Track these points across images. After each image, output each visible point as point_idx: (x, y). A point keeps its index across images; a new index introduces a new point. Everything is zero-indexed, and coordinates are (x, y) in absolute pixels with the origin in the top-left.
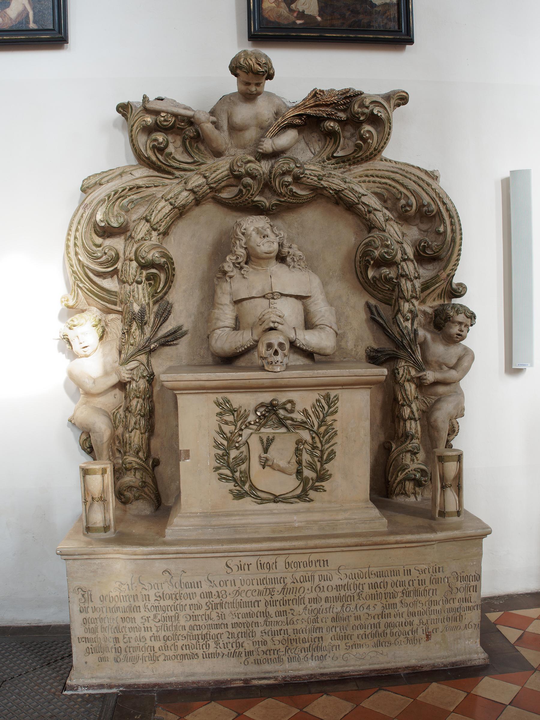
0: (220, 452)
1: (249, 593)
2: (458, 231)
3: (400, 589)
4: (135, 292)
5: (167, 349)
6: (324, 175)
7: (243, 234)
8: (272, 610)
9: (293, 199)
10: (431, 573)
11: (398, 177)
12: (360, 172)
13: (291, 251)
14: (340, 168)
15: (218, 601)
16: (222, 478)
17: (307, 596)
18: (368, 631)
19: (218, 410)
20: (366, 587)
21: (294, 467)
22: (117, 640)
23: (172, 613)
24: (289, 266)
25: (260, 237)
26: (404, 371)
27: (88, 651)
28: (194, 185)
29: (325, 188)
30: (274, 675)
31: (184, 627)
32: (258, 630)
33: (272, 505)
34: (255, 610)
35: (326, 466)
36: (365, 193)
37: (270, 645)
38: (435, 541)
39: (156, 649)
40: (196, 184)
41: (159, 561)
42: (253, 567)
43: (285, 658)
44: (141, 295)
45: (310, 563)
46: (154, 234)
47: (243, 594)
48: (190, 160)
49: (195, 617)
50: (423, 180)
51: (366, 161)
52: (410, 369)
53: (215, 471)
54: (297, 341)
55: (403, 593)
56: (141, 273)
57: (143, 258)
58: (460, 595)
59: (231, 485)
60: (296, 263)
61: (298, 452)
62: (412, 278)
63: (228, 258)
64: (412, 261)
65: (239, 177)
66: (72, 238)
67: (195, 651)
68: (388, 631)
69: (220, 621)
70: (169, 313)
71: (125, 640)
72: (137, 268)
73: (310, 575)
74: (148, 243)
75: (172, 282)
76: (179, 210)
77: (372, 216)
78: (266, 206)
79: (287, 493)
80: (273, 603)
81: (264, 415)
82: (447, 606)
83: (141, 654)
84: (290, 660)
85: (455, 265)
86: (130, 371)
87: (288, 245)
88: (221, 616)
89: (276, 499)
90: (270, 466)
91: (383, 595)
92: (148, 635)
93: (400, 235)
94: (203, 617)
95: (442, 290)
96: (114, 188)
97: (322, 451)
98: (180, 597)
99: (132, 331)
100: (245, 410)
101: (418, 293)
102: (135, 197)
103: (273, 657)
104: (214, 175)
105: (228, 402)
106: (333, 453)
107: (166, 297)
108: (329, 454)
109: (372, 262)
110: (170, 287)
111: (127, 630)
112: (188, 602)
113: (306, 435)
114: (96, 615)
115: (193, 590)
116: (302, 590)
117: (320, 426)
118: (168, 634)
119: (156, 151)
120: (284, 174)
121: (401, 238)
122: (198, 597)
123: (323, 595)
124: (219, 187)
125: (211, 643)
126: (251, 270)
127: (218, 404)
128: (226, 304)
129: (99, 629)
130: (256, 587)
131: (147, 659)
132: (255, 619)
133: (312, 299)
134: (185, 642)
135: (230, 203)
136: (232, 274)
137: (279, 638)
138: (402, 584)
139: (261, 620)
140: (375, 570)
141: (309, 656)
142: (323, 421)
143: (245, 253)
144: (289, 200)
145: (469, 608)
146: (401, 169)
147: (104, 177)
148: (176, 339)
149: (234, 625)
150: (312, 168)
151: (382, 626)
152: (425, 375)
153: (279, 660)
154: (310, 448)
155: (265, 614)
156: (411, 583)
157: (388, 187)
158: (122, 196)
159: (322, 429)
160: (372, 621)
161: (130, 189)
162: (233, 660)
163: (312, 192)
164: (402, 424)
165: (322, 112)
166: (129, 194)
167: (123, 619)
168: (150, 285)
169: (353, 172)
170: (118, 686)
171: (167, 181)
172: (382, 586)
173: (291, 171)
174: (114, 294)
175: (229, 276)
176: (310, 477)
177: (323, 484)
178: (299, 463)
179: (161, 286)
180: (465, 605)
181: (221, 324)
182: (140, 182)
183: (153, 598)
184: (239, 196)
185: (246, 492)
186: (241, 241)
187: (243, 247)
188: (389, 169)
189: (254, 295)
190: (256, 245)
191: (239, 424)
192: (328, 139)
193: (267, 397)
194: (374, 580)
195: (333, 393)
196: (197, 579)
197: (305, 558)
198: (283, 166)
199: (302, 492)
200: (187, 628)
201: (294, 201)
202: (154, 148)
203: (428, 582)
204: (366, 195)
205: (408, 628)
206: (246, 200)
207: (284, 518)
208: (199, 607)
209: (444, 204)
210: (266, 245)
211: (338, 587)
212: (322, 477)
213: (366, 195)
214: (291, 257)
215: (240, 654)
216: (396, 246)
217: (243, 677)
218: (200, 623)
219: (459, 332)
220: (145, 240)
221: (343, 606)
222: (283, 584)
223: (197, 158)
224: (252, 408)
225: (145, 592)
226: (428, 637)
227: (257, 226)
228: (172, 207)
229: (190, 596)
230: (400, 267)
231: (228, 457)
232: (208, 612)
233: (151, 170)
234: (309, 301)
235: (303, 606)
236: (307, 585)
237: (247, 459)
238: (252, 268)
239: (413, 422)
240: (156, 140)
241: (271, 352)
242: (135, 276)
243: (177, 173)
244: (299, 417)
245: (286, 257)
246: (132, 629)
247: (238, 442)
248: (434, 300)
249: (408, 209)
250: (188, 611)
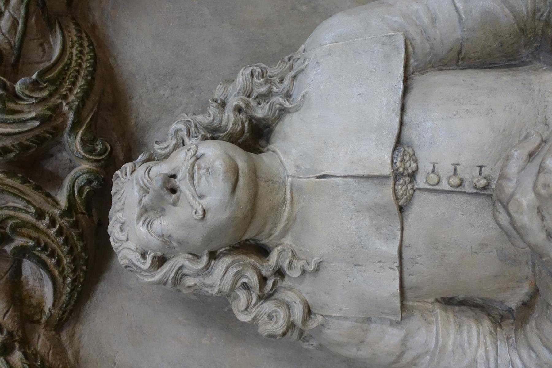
7: (160, 261)
9: (74, 84)
13: (233, 102)
24: (283, 111)
25: (175, 204)
60: (275, 89)
63: (244, 318)
78: (89, 172)
87: (213, 110)
126: (288, 241)
128: (404, 342)
133: (413, 32)
135: (74, 281)
143: (227, 260)
144: (71, 98)
163: (57, 28)
175: (305, 321)
184: (44, 256)
186: (185, 271)
187: (207, 267)
190: (200, 224)
201: (81, 82)
206: (60, 232)
214: (253, 103)
227: (137, 210)
238: (284, 233)
245: (251, 119)
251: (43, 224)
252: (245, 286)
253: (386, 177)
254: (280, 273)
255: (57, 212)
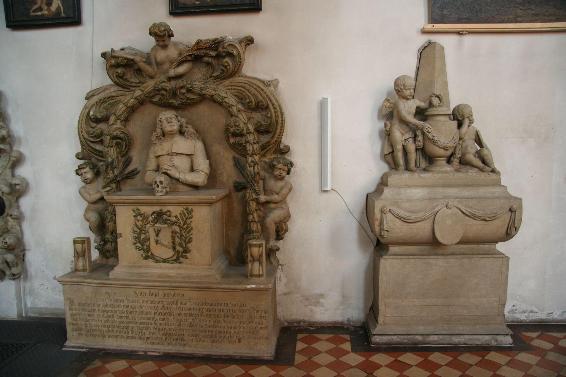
0: (136, 235)
1: (146, 308)
2: (280, 116)
3: (223, 313)
4: (109, 152)
5: (130, 180)
6: (204, 88)
7: (160, 121)
8: (158, 317)
10: (239, 306)
11: (246, 86)
12: (227, 83)
14: (216, 82)
15: (132, 310)
16: (138, 248)
17: (175, 312)
18: (207, 334)
19: (134, 214)
20: (204, 310)
21: (171, 245)
22: (86, 325)
23: (111, 314)
24: (185, 137)
26: (249, 195)
27: (74, 330)
28: (136, 95)
29: (204, 94)
30: (159, 351)
31: (117, 322)
32: (152, 327)
33: (162, 264)
34: (150, 316)
35: (188, 245)
36: (227, 96)
37: (158, 336)
38: (240, 289)
39: (104, 332)
40: (138, 95)
41: (104, 288)
42: (147, 294)
43: (165, 343)
44: (112, 153)
45: (175, 295)
46: (119, 121)
47: (144, 308)
48: (138, 81)
49: (121, 317)
50: (260, 88)
51: (230, 77)
52: (253, 194)
53: (134, 245)
54: (180, 179)
55: (224, 316)
56: (112, 142)
57: (112, 134)
58: (256, 320)
59: (142, 252)
61: (173, 238)
62: (252, 143)
63: (153, 134)
64: (253, 134)
65: (159, 90)
66: (80, 124)
67: (122, 334)
68: (218, 335)
69: (133, 321)
70: (130, 162)
71: (90, 326)
72: (110, 139)
73: (175, 300)
74: (114, 127)
75: (130, 146)
76: (131, 108)
77: (230, 109)
79: (169, 258)
80: (158, 314)
81: (155, 217)
82: (250, 325)
83: (98, 333)
84: (168, 344)
85: (279, 135)
86: (106, 192)
88: (134, 318)
89: (165, 261)
90: (159, 243)
91: (214, 316)
92: (100, 324)
93: (246, 119)
94: (125, 317)
95: (275, 149)
96: (100, 98)
97: (185, 237)
98: (114, 306)
99: (108, 171)
100: (147, 215)
101: (256, 152)
102: (111, 102)
103: (159, 341)
104: (146, 90)
105: (139, 210)
106: (191, 238)
107: (129, 153)
108: (189, 239)
109: (230, 135)
110: (129, 149)
111: (91, 320)
112: (118, 309)
113: (177, 229)
114: (77, 312)
115: (120, 303)
116: (172, 308)
117: (184, 224)
118: (110, 324)
119: (118, 78)
120: (182, 88)
121: (246, 121)
122: (122, 307)
123: (183, 312)
124: (150, 96)
125: (130, 331)
127: (134, 211)
129: (78, 320)
130: (149, 305)
131: (100, 336)
132: (150, 321)
133: (194, 156)
134: (117, 329)
136: (155, 142)
137: (162, 332)
138: (224, 311)
139: (153, 322)
140: (209, 302)
141: (177, 343)
142: (185, 222)
145: (262, 328)
146: (249, 81)
147: (97, 91)
148: (134, 175)
149: (140, 323)
150: (198, 83)
151: (214, 331)
152: (259, 198)
153: (162, 343)
154: (179, 236)
155: (154, 319)
156: (228, 311)
157: (241, 92)
158: (104, 102)
159: (185, 226)
160: (209, 329)
161: (108, 98)
162: (140, 341)
164: (249, 224)
165: (201, 53)
166: (108, 100)
167: (89, 315)
168: (118, 147)
169: (223, 84)
170: (87, 348)
171: (127, 93)
172: (213, 311)
173: (185, 86)
174: (102, 152)
176: (180, 251)
177: (187, 254)
178: (174, 243)
179: (124, 148)
180: (259, 326)
181: (149, 169)
182: (113, 94)
183: (102, 306)
185: (149, 256)
188: (243, 81)
189: (163, 154)
191: (145, 221)
192: (209, 67)
193: (157, 208)
194: (208, 307)
195: (190, 208)
196: (122, 298)
197: (172, 292)
198: (180, 84)
199: (177, 258)
200: (118, 322)
202: (117, 76)
203: (237, 311)
204: (227, 98)
205: (228, 335)
207: (166, 271)
208: (123, 312)
209: (271, 101)
210: (169, 127)
211: (190, 309)
212: (186, 251)
213: (227, 98)
215: (144, 338)
216: (242, 125)
217: (144, 350)
218: (124, 320)
219: (279, 174)
220: (114, 125)
221: (193, 319)
222: (162, 305)
223: (141, 80)
224: (150, 213)
225: (98, 303)
226: (239, 341)
228: (126, 107)
229: (119, 306)
230: (246, 137)
231: (140, 238)
232: (127, 315)
233: (119, 87)
234: (193, 157)
235: (173, 317)
236: (174, 306)
237: (148, 240)
239: (255, 223)
240: (117, 72)
241: (156, 185)
242: (109, 144)
243: (132, 89)
244: (173, 219)
246: (93, 320)
247: (144, 231)
248: (271, 155)
249: (250, 104)
250: (118, 314)
251: (165, 100)
252: (158, 134)
253: (171, 151)
254: (160, 139)
255: (167, 101)
